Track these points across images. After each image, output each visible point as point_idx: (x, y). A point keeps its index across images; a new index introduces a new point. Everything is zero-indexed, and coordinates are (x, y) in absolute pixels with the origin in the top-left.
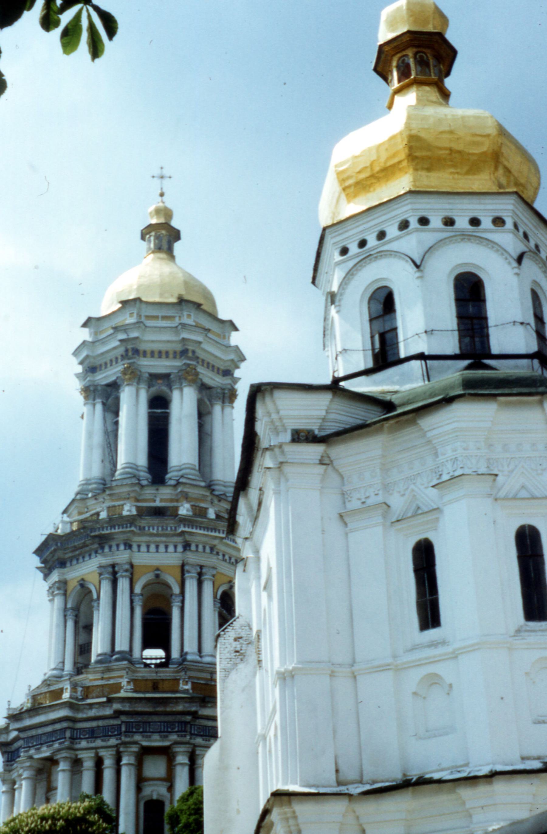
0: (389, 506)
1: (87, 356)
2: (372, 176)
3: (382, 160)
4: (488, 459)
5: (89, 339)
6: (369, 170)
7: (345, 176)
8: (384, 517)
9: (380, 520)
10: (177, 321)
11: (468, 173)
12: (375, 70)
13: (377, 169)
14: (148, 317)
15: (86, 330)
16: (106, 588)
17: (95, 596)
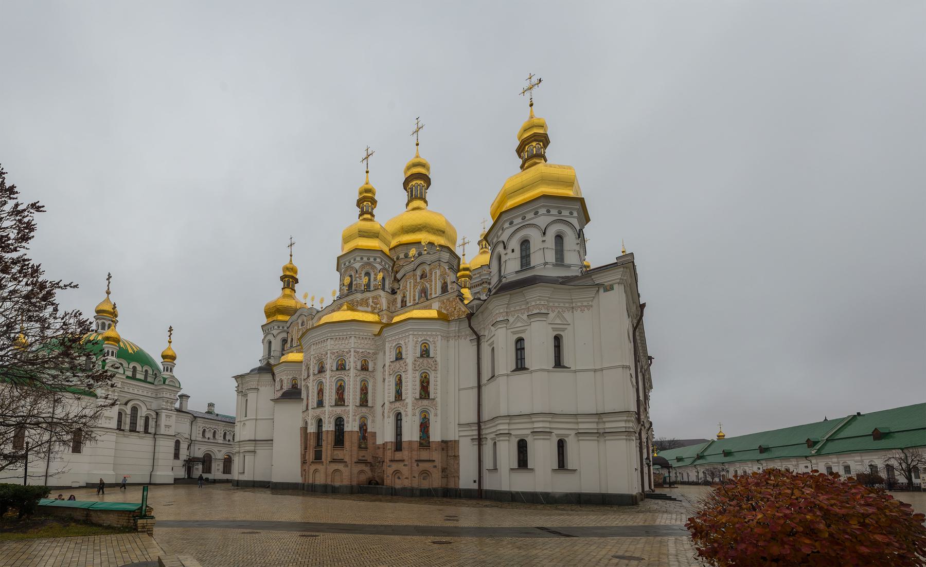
11: (274, 316)
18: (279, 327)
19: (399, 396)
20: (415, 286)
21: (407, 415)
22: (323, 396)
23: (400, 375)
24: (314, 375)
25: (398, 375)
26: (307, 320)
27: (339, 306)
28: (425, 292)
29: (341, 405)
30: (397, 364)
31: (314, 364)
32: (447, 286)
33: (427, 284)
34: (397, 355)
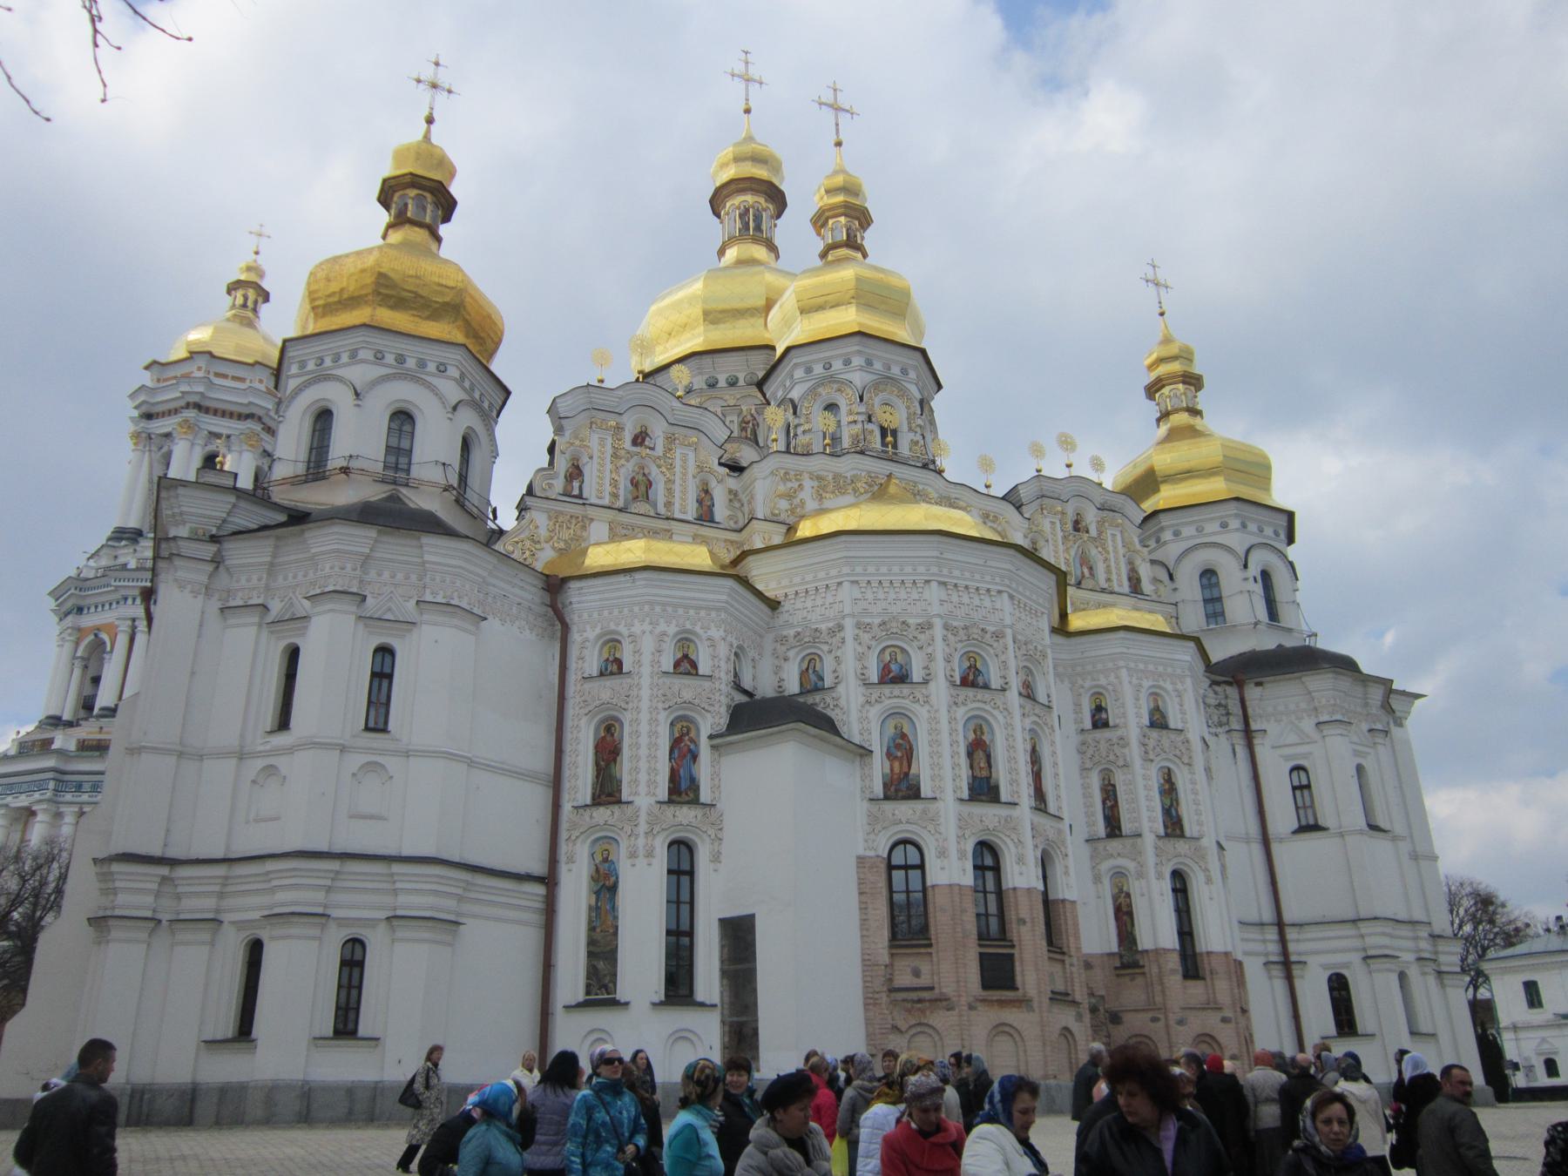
0: (268, 610)
1: (144, 402)
2: (339, 302)
3: (351, 289)
4: (361, 581)
5: (149, 384)
6: (337, 296)
7: (316, 296)
8: (262, 618)
9: (256, 619)
10: (248, 384)
11: (428, 318)
12: (379, 200)
13: (345, 296)
14: (217, 375)
15: (147, 374)
16: (122, 640)
17: (108, 649)
18: (462, 375)
19: (1174, 826)
20: (1065, 538)
21: (1209, 881)
22: (990, 766)
23: (1169, 769)
24: (953, 684)
25: (1164, 767)
26: (670, 439)
27: (863, 474)
28: (1091, 568)
29: (1040, 810)
30: (1166, 738)
31: (946, 649)
32: (1139, 580)
33: (1094, 552)
34: (1151, 714)
